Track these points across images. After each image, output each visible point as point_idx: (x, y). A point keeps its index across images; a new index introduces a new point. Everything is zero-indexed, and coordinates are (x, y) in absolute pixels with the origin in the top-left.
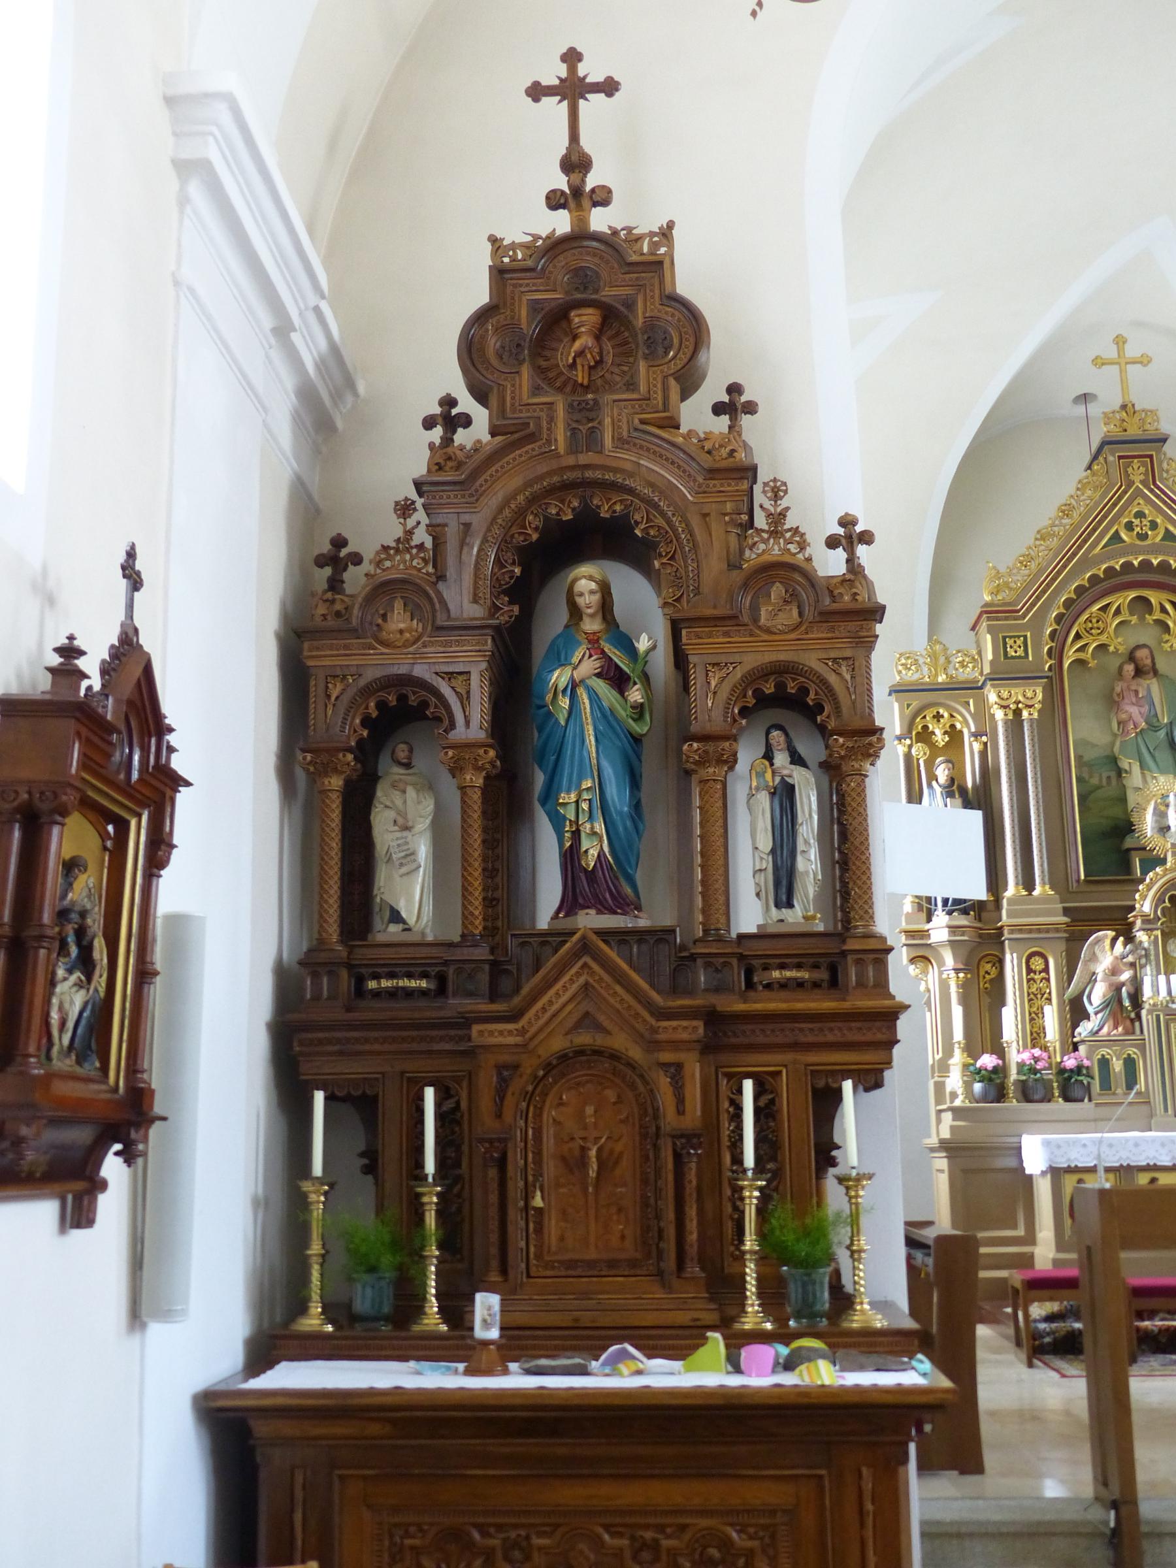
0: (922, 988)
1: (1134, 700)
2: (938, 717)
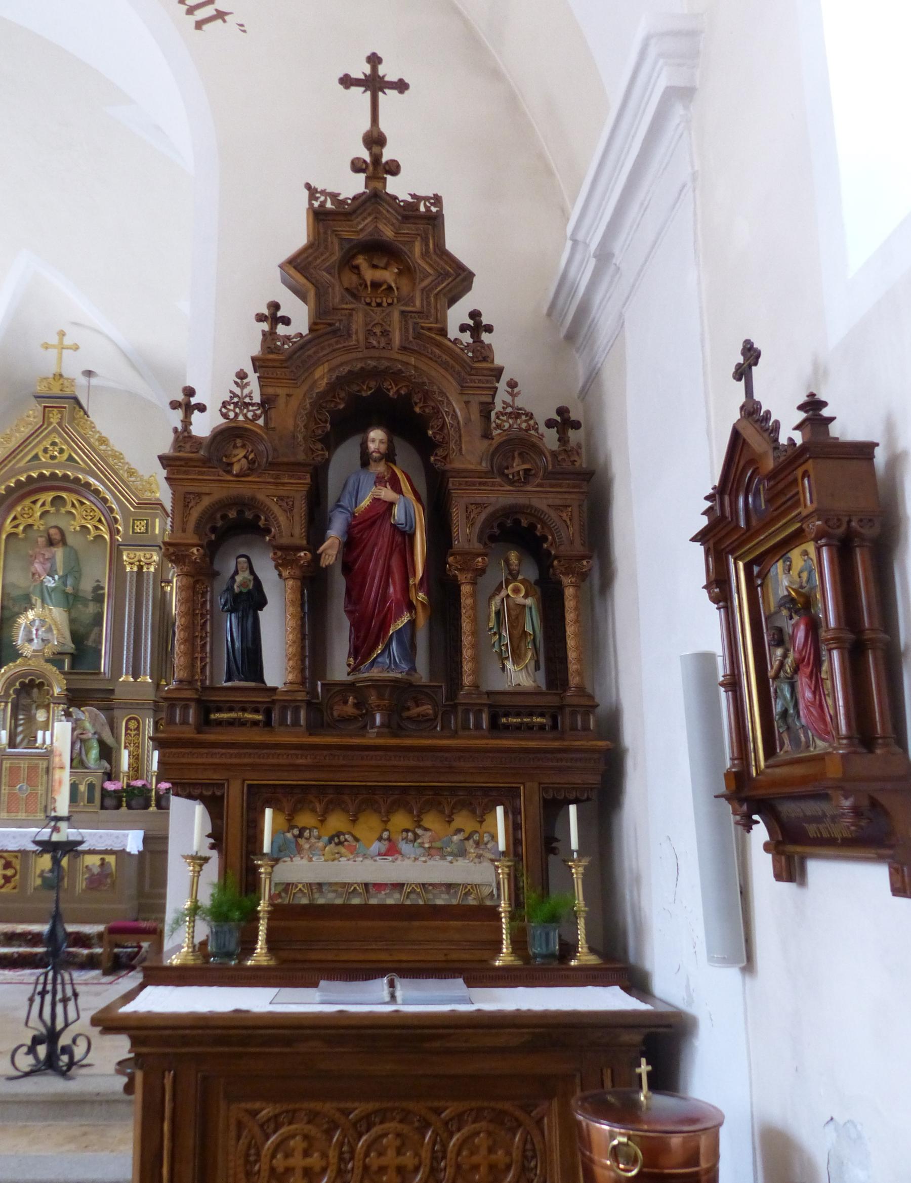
1: (42, 560)
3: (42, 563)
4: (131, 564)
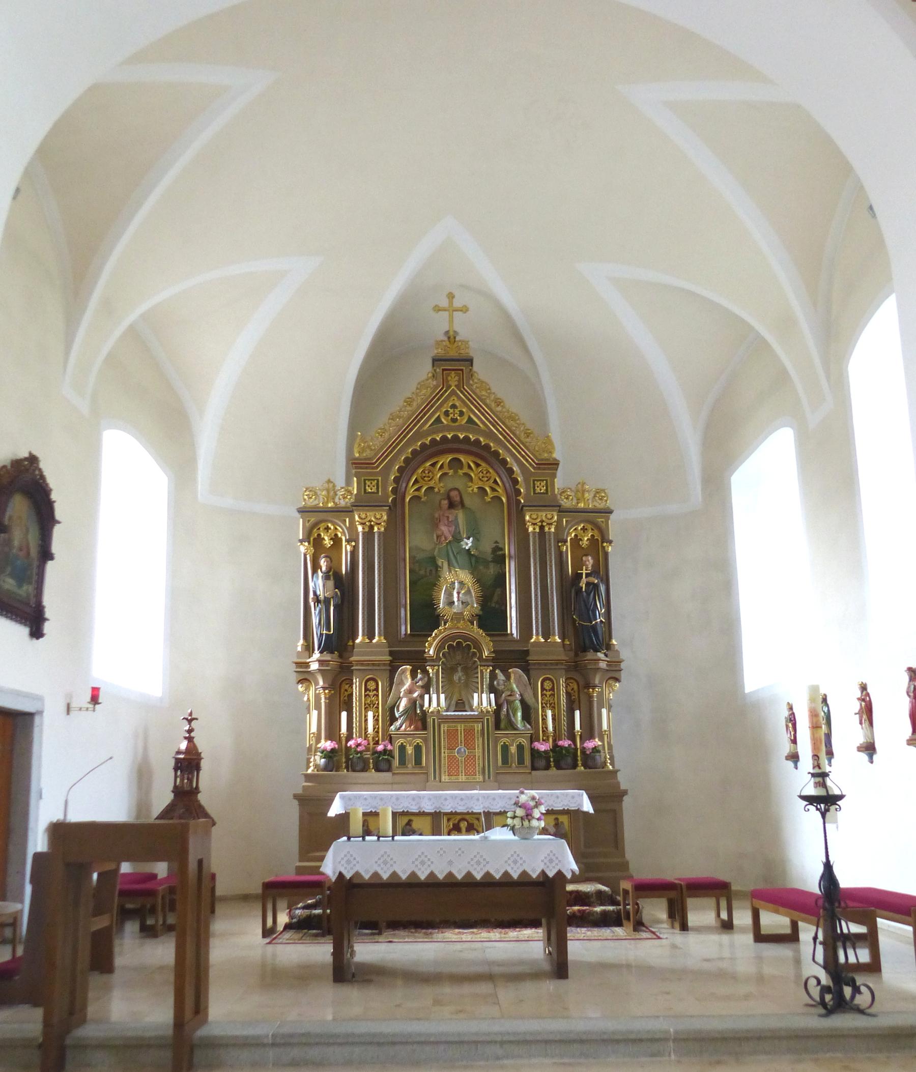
0: (305, 699)
2: (327, 529)
3: (448, 526)
4: (534, 524)
